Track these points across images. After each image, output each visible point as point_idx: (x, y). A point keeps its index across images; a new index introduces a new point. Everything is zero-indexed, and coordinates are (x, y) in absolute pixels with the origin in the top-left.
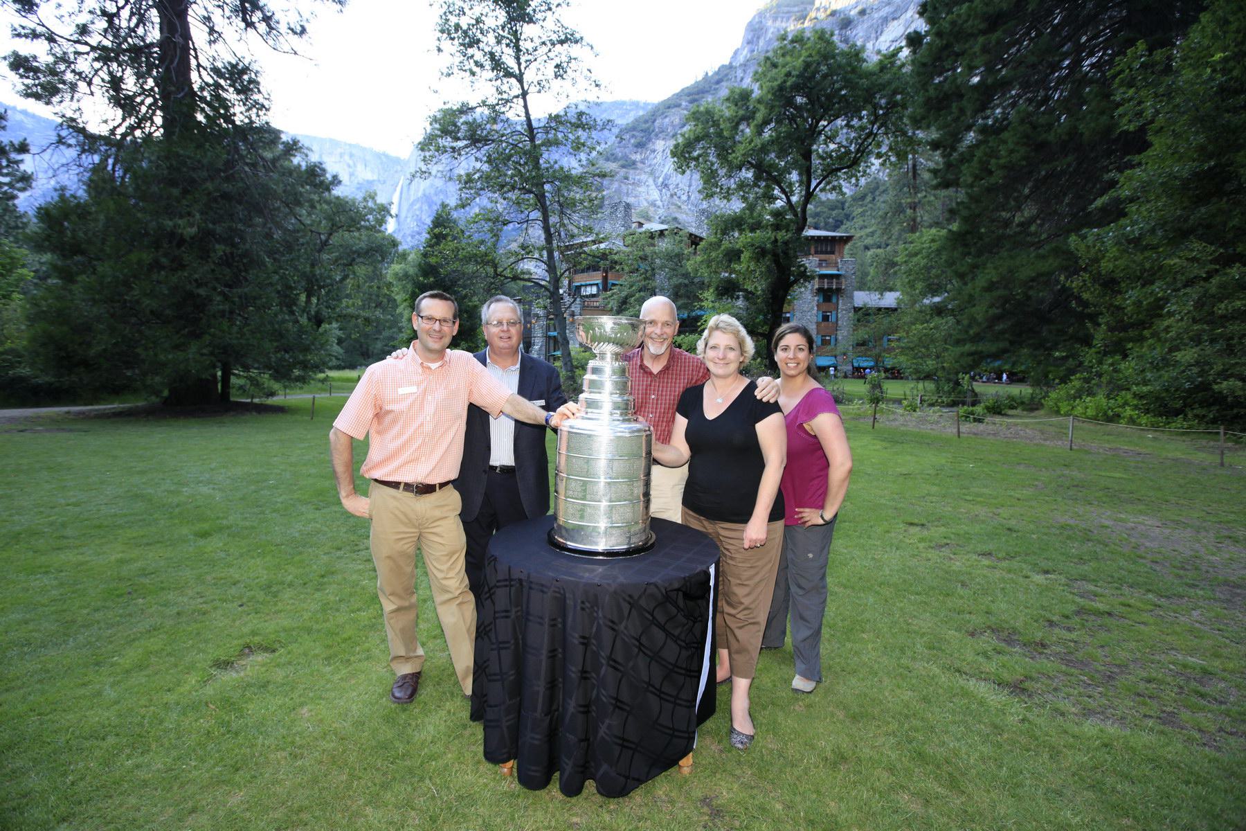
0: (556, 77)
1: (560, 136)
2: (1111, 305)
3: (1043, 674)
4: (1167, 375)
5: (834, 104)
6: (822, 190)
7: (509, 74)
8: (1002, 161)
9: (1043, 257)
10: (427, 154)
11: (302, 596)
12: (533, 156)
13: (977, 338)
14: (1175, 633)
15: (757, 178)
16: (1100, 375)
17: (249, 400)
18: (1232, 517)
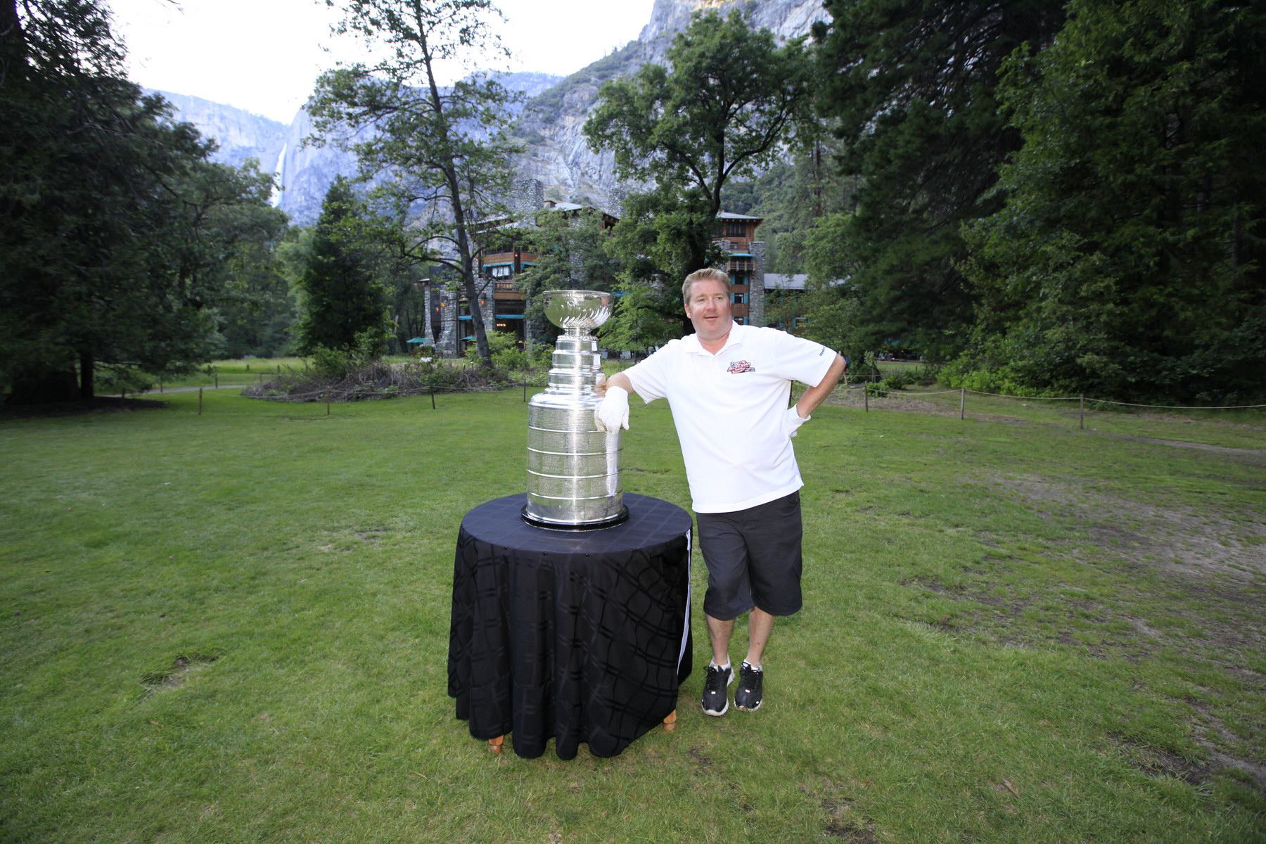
0: (463, 42)
1: (468, 106)
2: (993, 287)
5: (745, 88)
6: (734, 173)
7: (409, 35)
8: (900, 151)
9: (936, 242)
10: (318, 119)
11: (234, 601)
12: (441, 127)
13: (880, 318)
15: (672, 158)
16: (984, 352)
17: (119, 396)
18: (1093, 471)
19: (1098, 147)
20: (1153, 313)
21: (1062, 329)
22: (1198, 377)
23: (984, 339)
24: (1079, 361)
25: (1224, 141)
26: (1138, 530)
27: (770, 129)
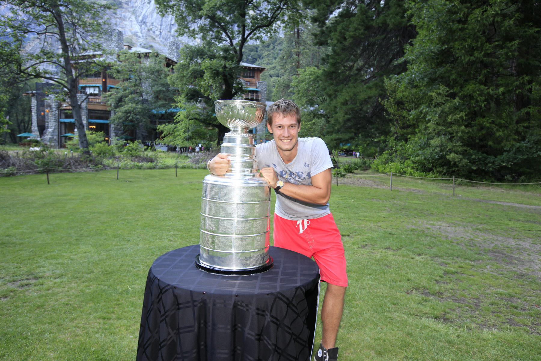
2: (401, 116)
3: (451, 309)
4: (428, 152)
6: (251, 38)
8: (352, 34)
9: (370, 88)
13: (338, 131)
14: (486, 278)
15: (212, 25)
16: (396, 151)
18: (472, 220)
19: (456, 40)
20: (484, 132)
21: (439, 139)
22: (505, 167)
23: (396, 145)
24: (448, 157)
25: (517, 42)
26: (512, 253)
27: (274, 13)
